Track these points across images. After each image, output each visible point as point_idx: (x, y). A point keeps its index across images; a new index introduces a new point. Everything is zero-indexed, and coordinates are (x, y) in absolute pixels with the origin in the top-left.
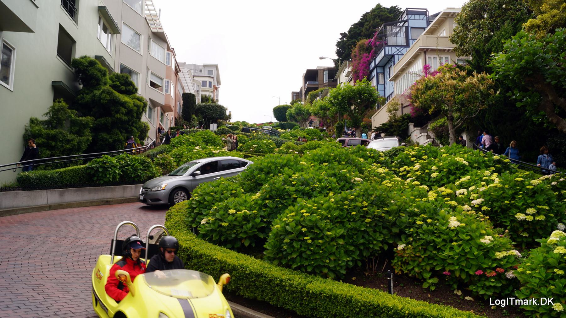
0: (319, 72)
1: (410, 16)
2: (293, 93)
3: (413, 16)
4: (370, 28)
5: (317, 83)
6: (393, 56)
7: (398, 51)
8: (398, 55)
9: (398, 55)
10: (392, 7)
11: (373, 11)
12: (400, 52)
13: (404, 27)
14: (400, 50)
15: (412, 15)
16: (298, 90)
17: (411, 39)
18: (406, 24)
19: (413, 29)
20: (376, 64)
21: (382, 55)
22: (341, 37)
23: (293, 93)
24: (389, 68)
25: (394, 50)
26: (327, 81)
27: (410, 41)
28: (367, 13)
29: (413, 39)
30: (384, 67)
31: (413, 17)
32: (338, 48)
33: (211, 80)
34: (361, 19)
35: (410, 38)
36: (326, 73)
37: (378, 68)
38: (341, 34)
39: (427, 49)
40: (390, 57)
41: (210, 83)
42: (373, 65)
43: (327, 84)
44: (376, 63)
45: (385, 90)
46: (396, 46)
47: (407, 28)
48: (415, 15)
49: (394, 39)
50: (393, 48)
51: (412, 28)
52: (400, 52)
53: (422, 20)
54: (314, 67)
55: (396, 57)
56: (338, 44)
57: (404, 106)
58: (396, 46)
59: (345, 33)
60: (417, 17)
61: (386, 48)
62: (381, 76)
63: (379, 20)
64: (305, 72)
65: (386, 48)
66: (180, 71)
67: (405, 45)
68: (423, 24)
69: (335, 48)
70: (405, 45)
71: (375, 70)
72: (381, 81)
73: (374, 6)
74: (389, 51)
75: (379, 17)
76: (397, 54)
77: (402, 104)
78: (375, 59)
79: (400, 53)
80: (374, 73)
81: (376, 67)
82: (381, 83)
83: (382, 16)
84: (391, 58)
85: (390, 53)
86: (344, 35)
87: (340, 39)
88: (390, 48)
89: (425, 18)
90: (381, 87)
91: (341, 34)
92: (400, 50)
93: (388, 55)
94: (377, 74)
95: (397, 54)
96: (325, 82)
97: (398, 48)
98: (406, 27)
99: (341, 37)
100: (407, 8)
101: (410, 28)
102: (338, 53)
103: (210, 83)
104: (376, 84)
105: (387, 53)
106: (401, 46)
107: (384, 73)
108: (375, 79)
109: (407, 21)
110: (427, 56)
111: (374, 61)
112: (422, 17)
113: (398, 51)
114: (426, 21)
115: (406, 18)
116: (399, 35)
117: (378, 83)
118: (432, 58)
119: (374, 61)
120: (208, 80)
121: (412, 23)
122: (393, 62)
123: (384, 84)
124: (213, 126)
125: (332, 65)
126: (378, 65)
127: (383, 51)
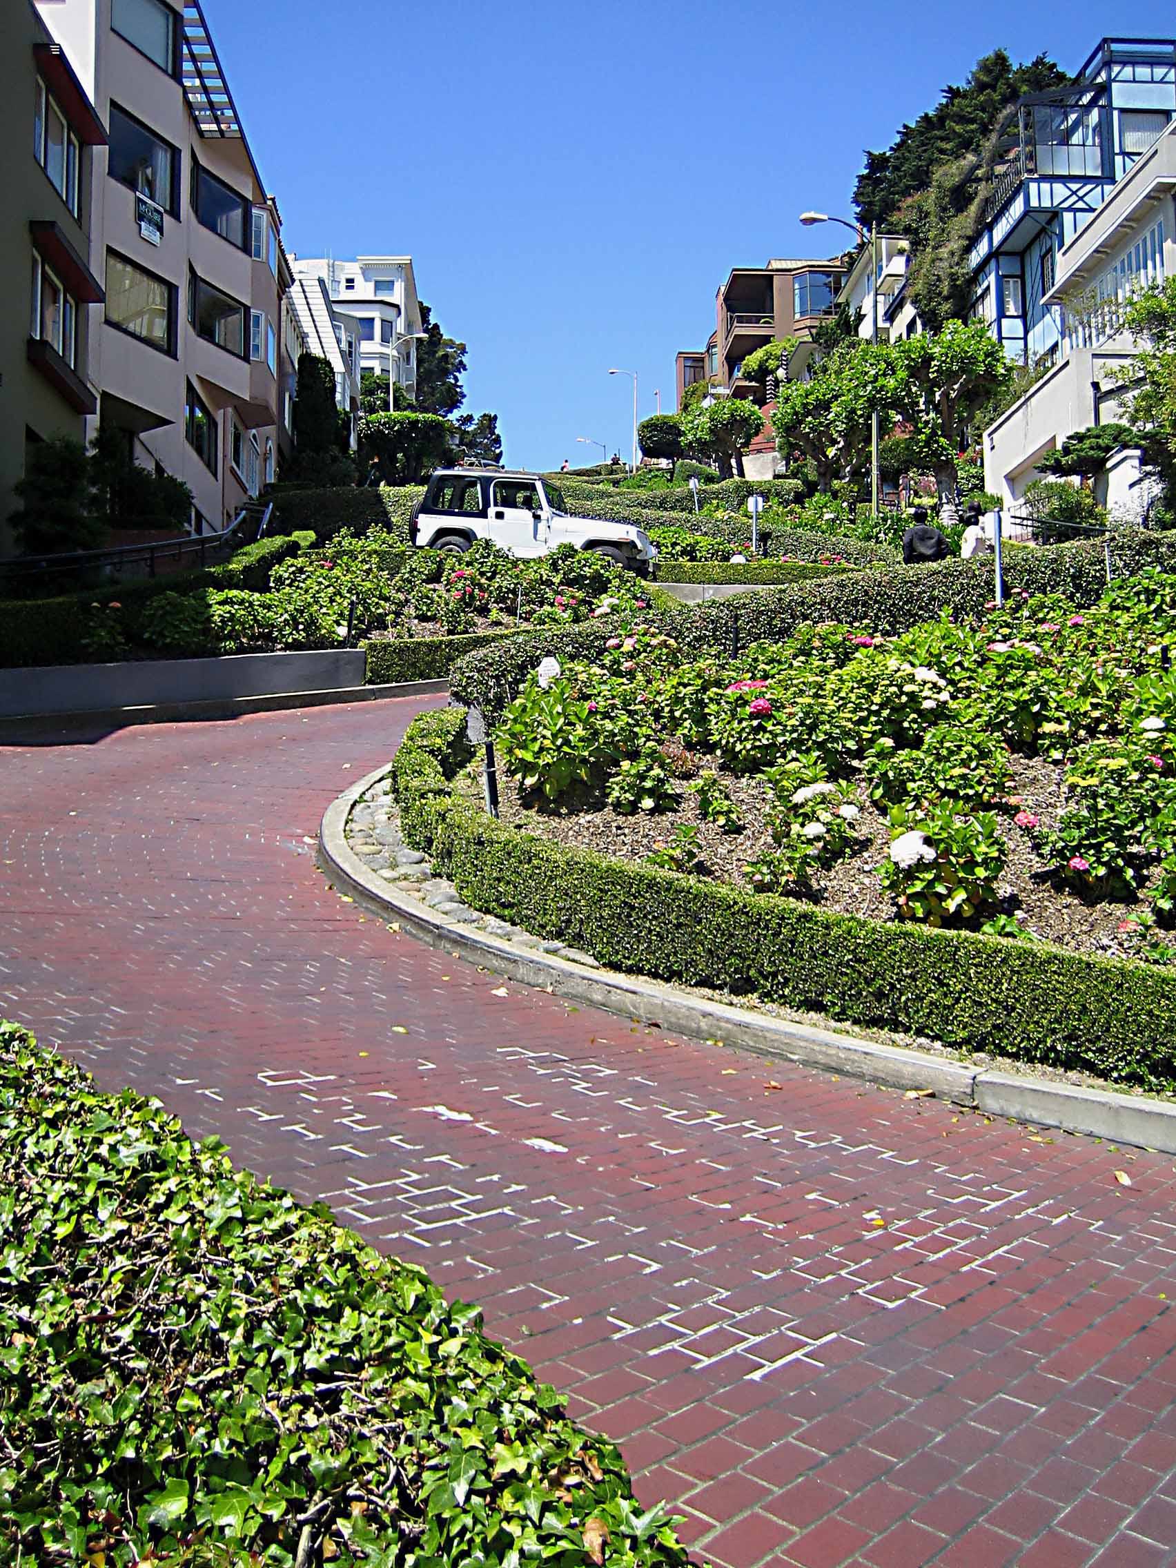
1: (1116, 69)
6: (1055, 215)
7: (1074, 198)
12: (1081, 199)
14: (1081, 193)
15: (1124, 64)
17: (1124, 154)
19: (1125, 116)
21: (1017, 208)
24: (1043, 258)
25: (1060, 190)
27: (1118, 160)
29: (1129, 154)
30: (1021, 255)
31: (1128, 70)
33: (390, 314)
35: (1117, 150)
37: (1001, 259)
40: (1043, 218)
41: (387, 325)
44: (996, 243)
46: (1064, 179)
50: (1058, 187)
51: (1123, 111)
52: (1081, 199)
53: (1161, 82)
55: (1068, 217)
58: (1064, 179)
60: (1143, 72)
61: (1033, 187)
66: (293, 281)
74: (1042, 195)
76: (1069, 209)
77: (1096, 386)
78: (990, 228)
79: (1080, 205)
81: (993, 255)
84: (1049, 222)
85: (1046, 203)
88: (1045, 187)
92: (1081, 193)
94: (1000, 279)
95: (1069, 209)
97: (1074, 187)
100: (1105, 41)
101: (1116, 113)
103: (387, 325)
104: (994, 316)
105: (1034, 203)
106: (1085, 179)
107: (1022, 277)
108: (991, 301)
113: (1074, 198)
116: (1076, 138)
117: (1002, 314)
120: (375, 313)
126: (1003, 249)
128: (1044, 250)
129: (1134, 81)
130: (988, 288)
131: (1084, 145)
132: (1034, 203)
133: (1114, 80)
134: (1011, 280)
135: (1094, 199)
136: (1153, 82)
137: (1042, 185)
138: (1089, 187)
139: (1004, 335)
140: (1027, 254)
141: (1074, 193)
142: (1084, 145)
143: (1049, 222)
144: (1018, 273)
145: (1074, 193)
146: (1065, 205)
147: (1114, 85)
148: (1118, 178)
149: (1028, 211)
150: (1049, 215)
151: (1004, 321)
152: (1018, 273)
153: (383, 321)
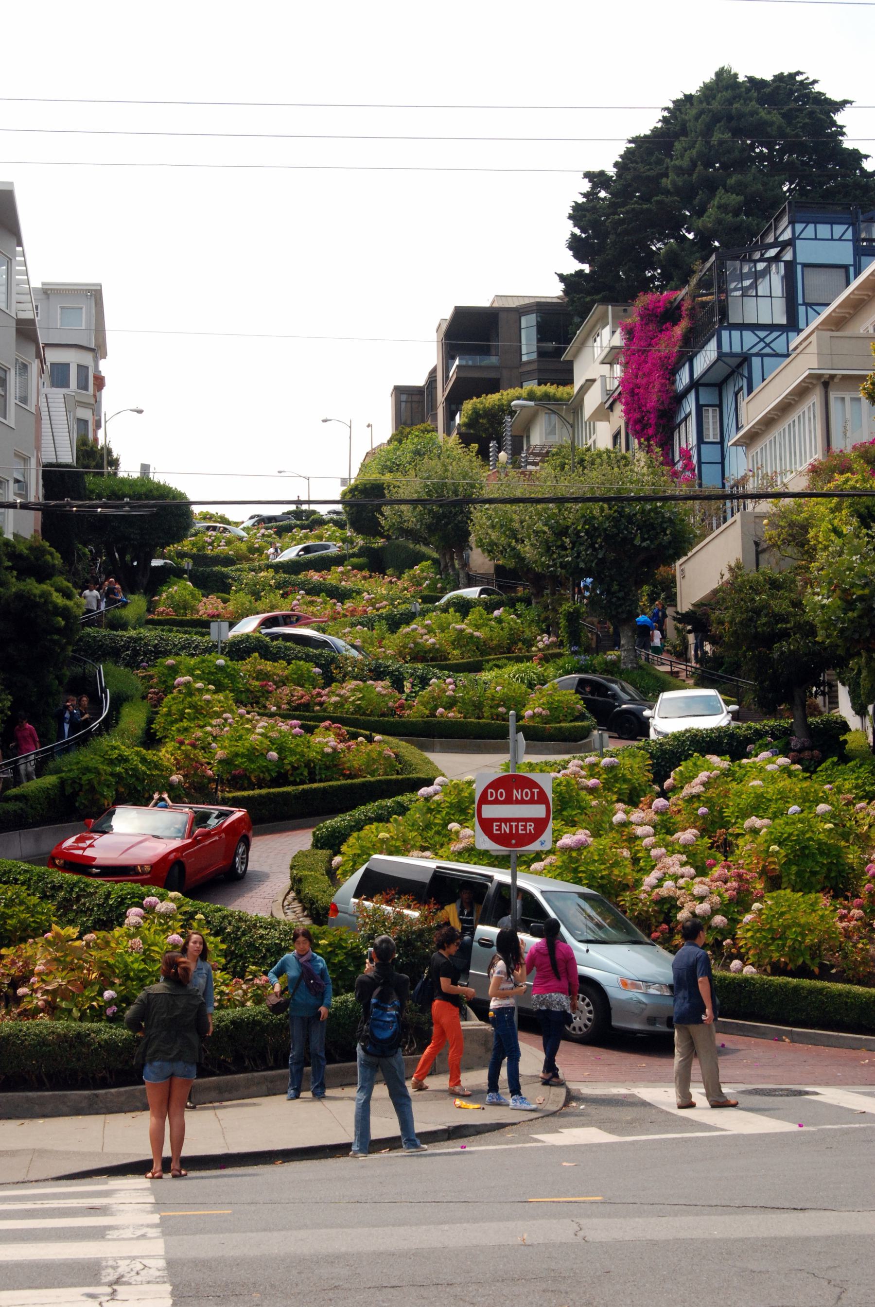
0: (502, 316)
1: (799, 227)
2: (399, 391)
3: (811, 227)
4: (694, 165)
5: (493, 360)
6: (745, 359)
7: (762, 345)
8: (763, 356)
9: (763, 356)
10: (780, 78)
11: (709, 91)
12: (768, 345)
13: (782, 264)
14: (768, 340)
15: (808, 223)
16: (420, 381)
17: (805, 304)
18: (788, 256)
19: (806, 270)
20: (695, 376)
22: (586, 186)
23: (399, 391)
24: (736, 394)
25: (750, 338)
26: (534, 356)
27: (802, 310)
28: (689, 98)
30: (719, 386)
32: (577, 231)
33: (86, 359)
34: (665, 120)
35: (800, 301)
36: (528, 322)
37: (701, 389)
38: (588, 175)
39: (832, 377)
40: (734, 362)
42: (683, 379)
43: (534, 366)
44: (697, 373)
45: (722, 463)
47: (790, 267)
48: (815, 223)
49: (750, 302)
50: (747, 334)
51: (805, 266)
52: (768, 345)
53: (840, 239)
54: (482, 299)
55: (756, 362)
56: (578, 214)
57: (764, 545)
59: (602, 173)
60: (824, 230)
61: (725, 334)
62: (711, 416)
63: (727, 136)
64: (448, 314)
65: (725, 334)
67: (784, 321)
68: (844, 253)
69: (569, 229)
70: (784, 321)
71: (692, 397)
72: (711, 435)
73: (709, 76)
75: (730, 118)
76: (757, 355)
77: (757, 544)
79: (767, 350)
80: (690, 405)
81: (695, 385)
82: (711, 439)
83: (741, 115)
84: (740, 365)
85: (737, 349)
86: (597, 179)
87: (585, 195)
88: (736, 334)
89: (849, 235)
90: (710, 453)
91: (588, 175)
92: (768, 340)
93: (732, 355)
94: (699, 408)
95: (757, 355)
96: (525, 358)
97: (762, 334)
98: (786, 262)
99: (586, 186)
101: (799, 268)
102: (577, 247)
103: (82, 369)
104: (693, 440)
105: (726, 348)
106: (772, 327)
107: (720, 406)
108: (692, 422)
109: (791, 243)
110: (833, 395)
111: (687, 366)
112: (839, 229)
113: (762, 345)
114: (850, 245)
115: (787, 235)
116: (763, 289)
118: (847, 400)
119: (687, 366)
121: (806, 252)
122: (745, 380)
123: (722, 443)
124: (219, 628)
125: (554, 290)
126: (701, 382)
127: (713, 344)
128: (736, 389)
129: (816, 239)
130: (690, 413)
131: (771, 296)
132: (726, 348)
133: (798, 238)
134: (710, 409)
135: (779, 345)
136: (832, 239)
137: (733, 332)
138: (775, 334)
139: (703, 460)
140: (724, 386)
141: (762, 340)
142: (771, 296)
143: (740, 365)
144: (718, 403)
145: (762, 340)
146: (755, 350)
147: (798, 242)
148: (802, 324)
149: (721, 356)
150: (739, 360)
151: (702, 446)
152: (718, 403)
153: (78, 365)
